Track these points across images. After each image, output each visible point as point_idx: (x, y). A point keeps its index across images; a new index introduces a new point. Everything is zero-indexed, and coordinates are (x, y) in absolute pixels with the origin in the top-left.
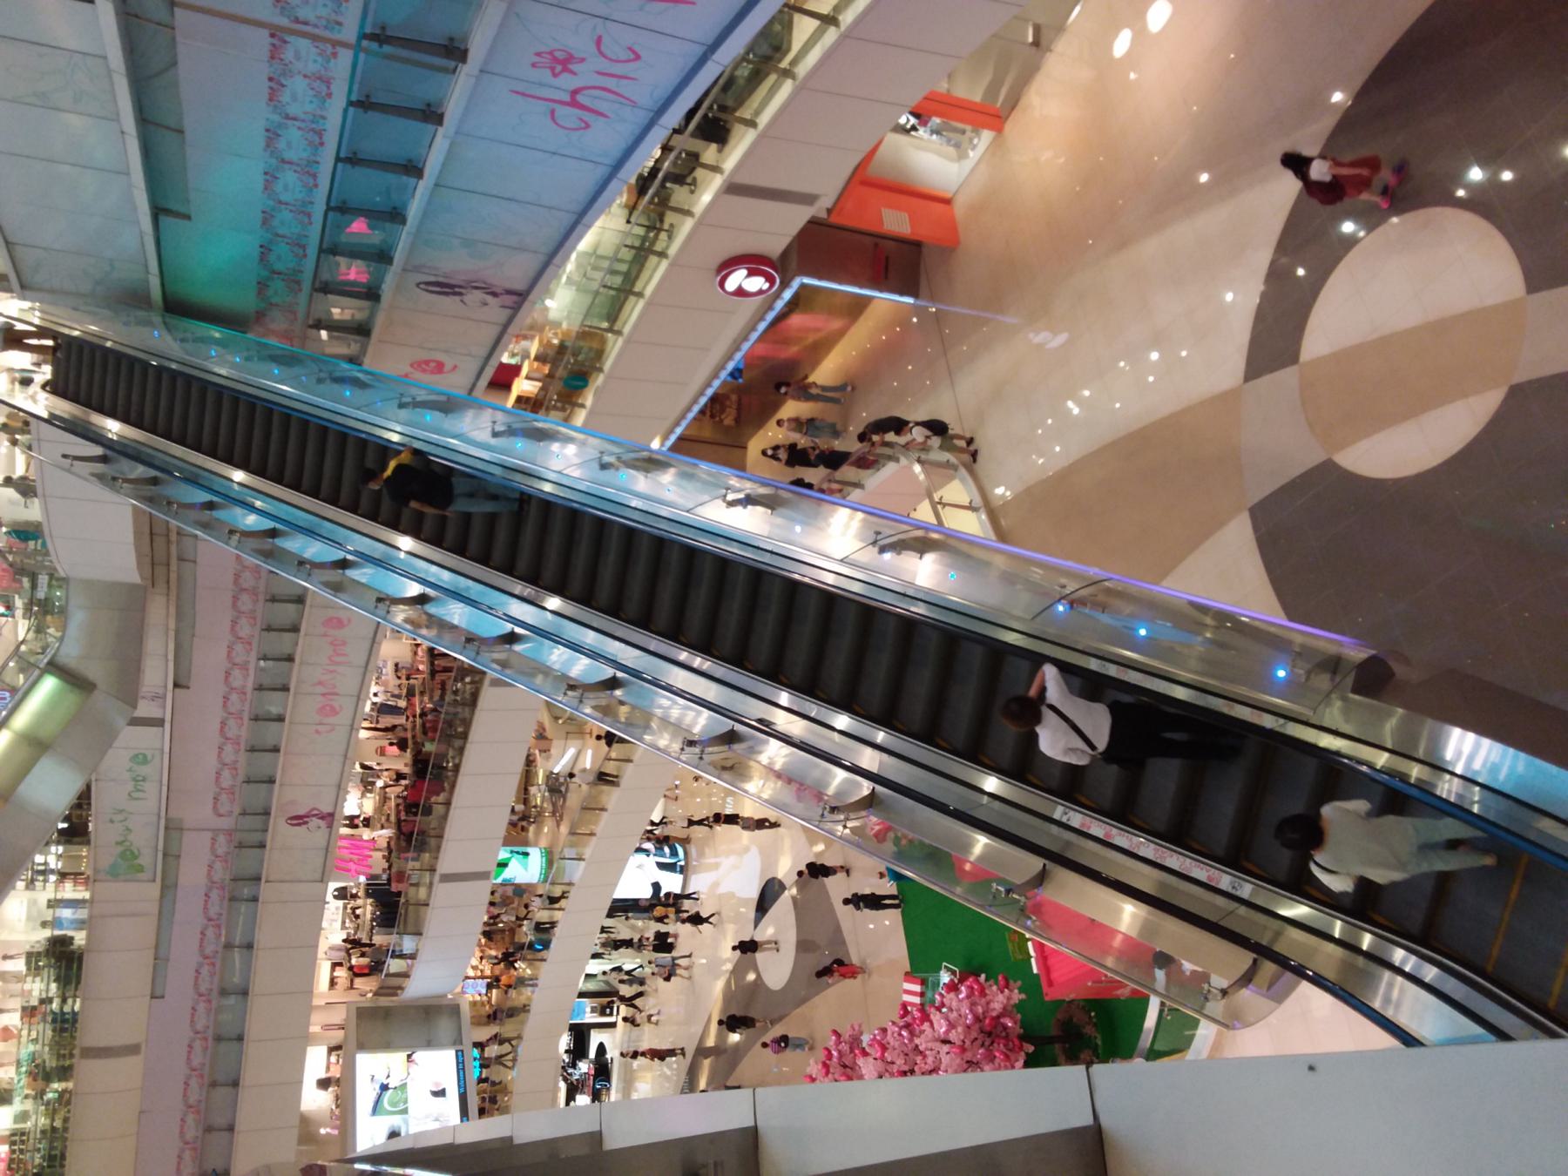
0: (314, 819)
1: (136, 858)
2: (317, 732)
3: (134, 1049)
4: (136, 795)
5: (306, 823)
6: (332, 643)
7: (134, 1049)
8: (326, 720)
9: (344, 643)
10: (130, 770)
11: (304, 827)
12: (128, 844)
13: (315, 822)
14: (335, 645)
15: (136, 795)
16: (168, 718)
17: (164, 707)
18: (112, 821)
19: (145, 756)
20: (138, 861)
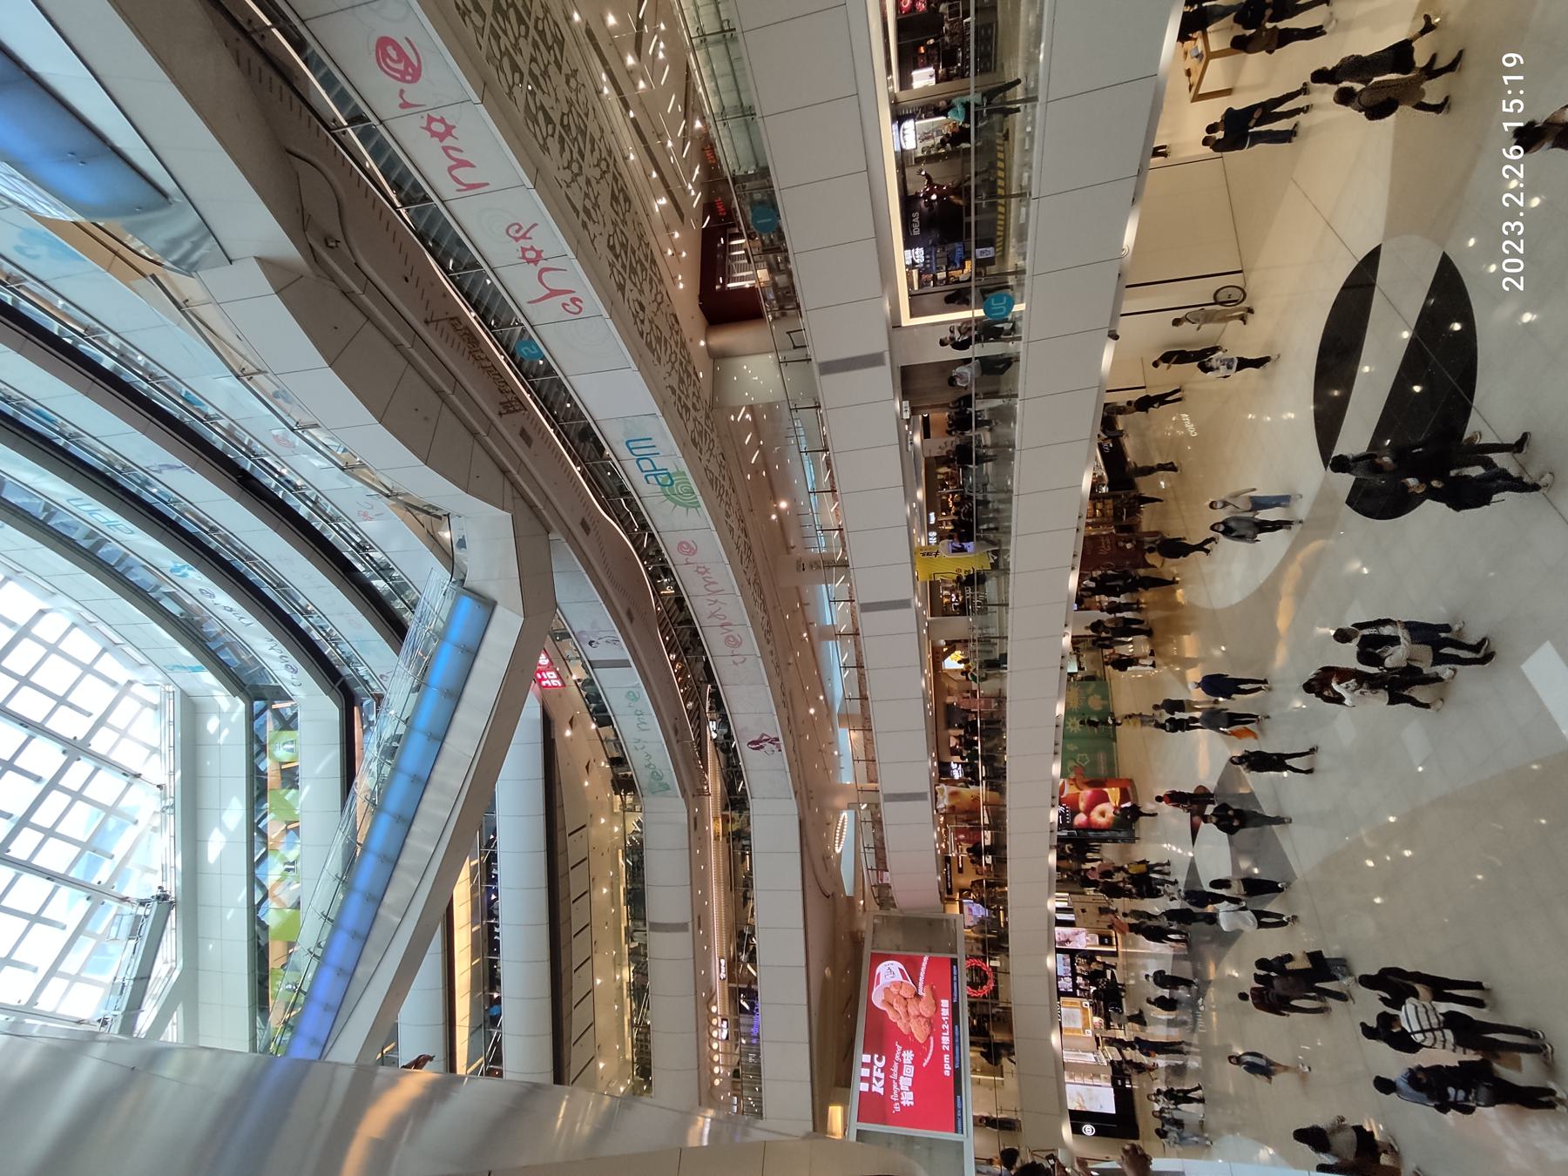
4: (643, 726)
5: (762, 747)
13: (768, 746)
15: (643, 726)
20: (664, 781)
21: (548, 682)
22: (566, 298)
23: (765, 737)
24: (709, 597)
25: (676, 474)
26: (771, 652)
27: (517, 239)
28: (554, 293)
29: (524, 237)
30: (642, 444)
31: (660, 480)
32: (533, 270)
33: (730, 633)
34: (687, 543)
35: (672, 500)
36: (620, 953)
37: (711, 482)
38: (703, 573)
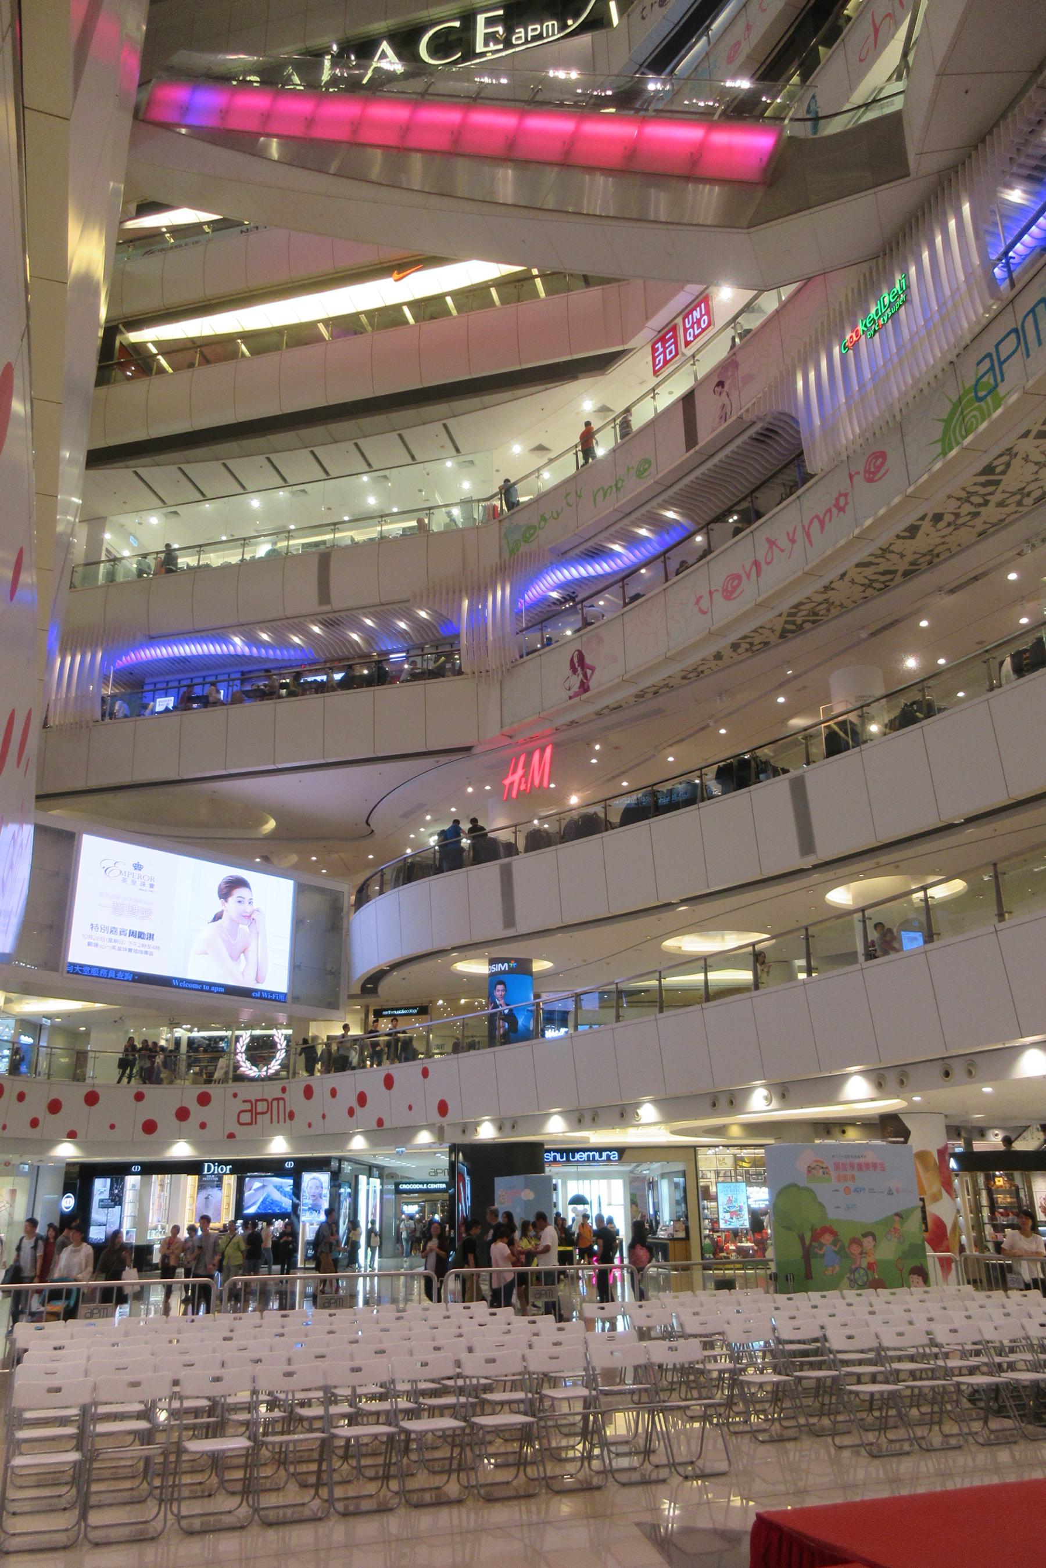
0: (581, 676)
1: (525, 541)
4: (601, 494)
5: (574, 671)
8: (718, 597)
11: (569, 672)
12: (542, 523)
13: (576, 681)
21: (661, 350)
23: (589, 672)
24: (799, 529)
26: (718, 656)
31: (985, 379)
34: (883, 464)
35: (953, 412)
36: (289, 534)
37: (989, 470)
38: (837, 505)
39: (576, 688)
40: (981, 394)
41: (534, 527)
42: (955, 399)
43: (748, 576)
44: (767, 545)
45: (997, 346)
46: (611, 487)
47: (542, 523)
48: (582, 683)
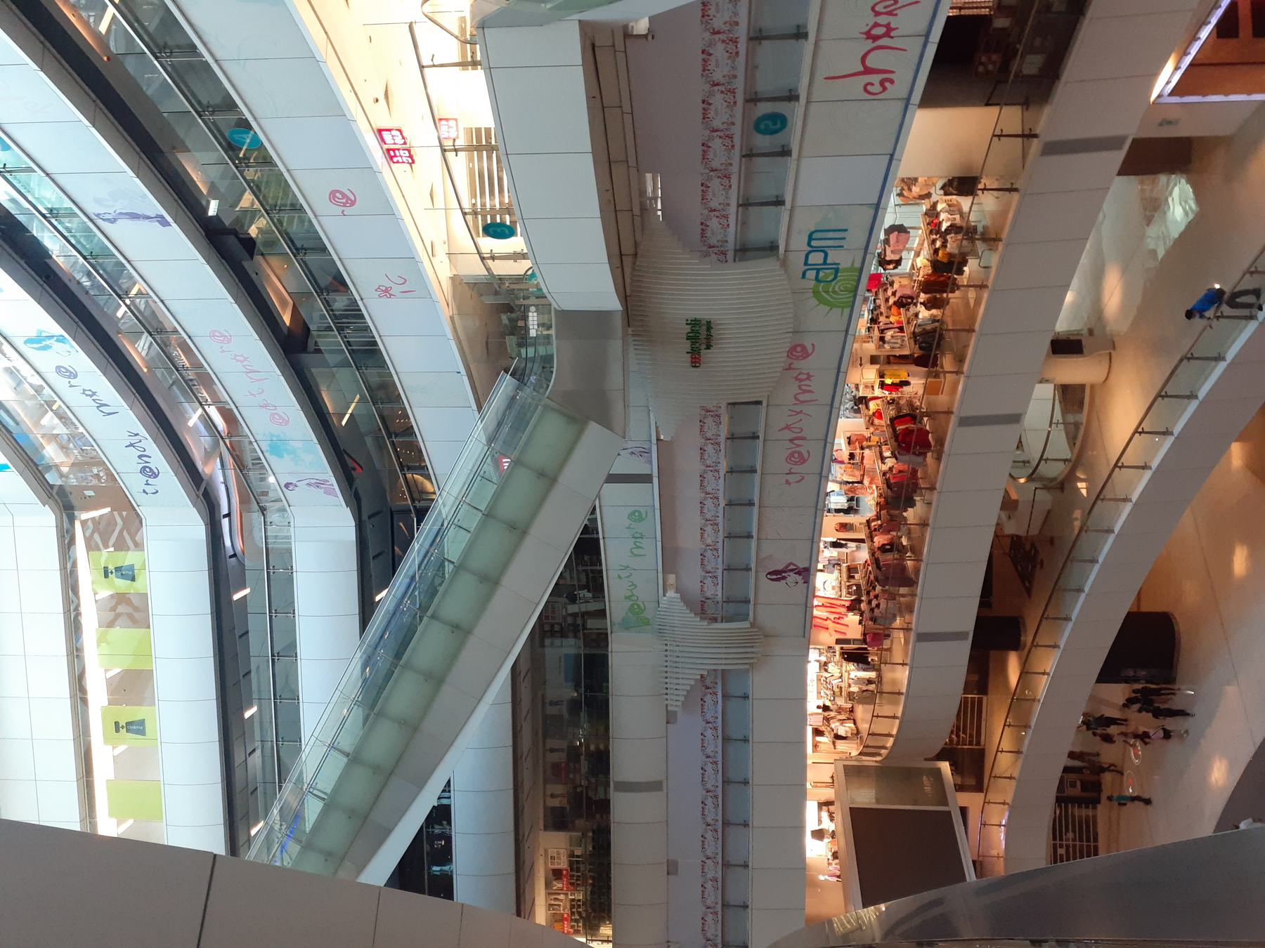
0: (791, 574)
2: (788, 482)
3: (655, 786)
5: (784, 578)
6: (797, 379)
7: (655, 786)
8: (796, 469)
9: (809, 377)
10: (629, 528)
11: (783, 582)
12: (633, 598)
13: (792, 577)
14: (801, 380)
16: (655, 473)
17: (651, 462)
18: (619, 577)
19: (639, 512)
22: (876, 79)
25: (847, 270)
27: (877, 14)
28: (868, 71)
29: (890, 13)
30: (831, 235)
32: (869, 44)
33: (798, 449)
39: (799, 578)
40: (832, 277)
41: (632, 605)
42: (812, 294)
43: (798, 446)
44: (786, 431)
45: (806, 264)
46: (635, 543)
47: (633, 598)
48: (799, 573)
